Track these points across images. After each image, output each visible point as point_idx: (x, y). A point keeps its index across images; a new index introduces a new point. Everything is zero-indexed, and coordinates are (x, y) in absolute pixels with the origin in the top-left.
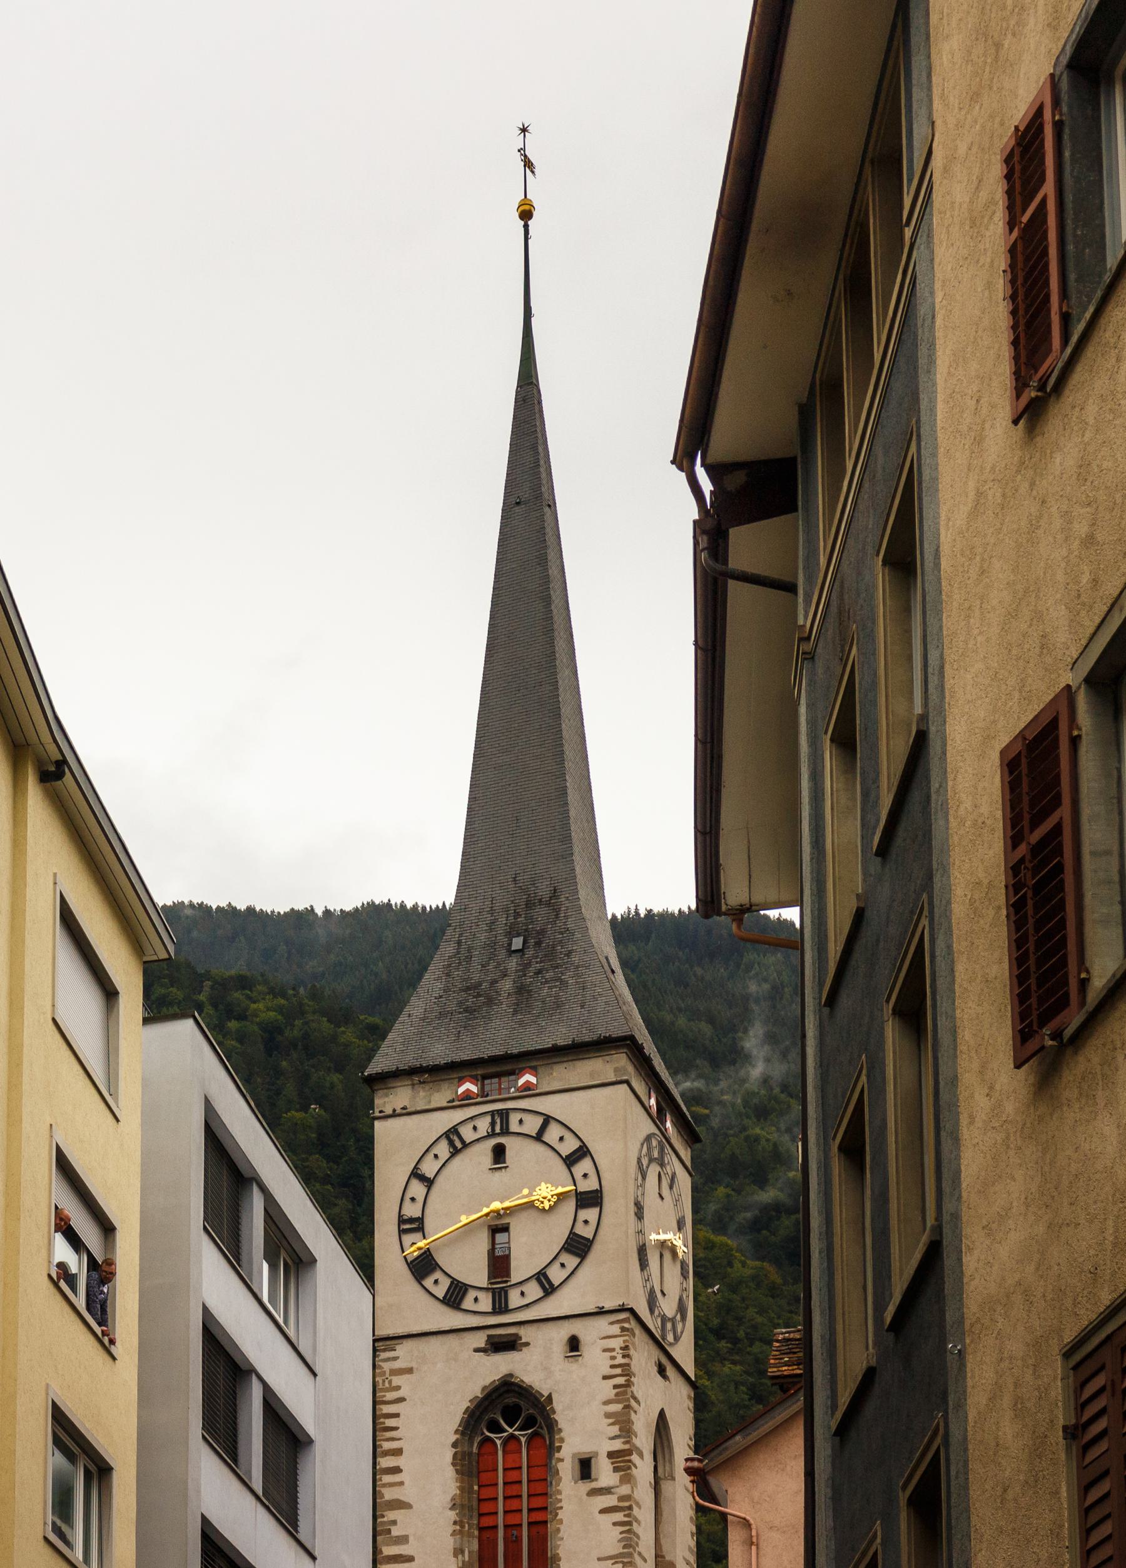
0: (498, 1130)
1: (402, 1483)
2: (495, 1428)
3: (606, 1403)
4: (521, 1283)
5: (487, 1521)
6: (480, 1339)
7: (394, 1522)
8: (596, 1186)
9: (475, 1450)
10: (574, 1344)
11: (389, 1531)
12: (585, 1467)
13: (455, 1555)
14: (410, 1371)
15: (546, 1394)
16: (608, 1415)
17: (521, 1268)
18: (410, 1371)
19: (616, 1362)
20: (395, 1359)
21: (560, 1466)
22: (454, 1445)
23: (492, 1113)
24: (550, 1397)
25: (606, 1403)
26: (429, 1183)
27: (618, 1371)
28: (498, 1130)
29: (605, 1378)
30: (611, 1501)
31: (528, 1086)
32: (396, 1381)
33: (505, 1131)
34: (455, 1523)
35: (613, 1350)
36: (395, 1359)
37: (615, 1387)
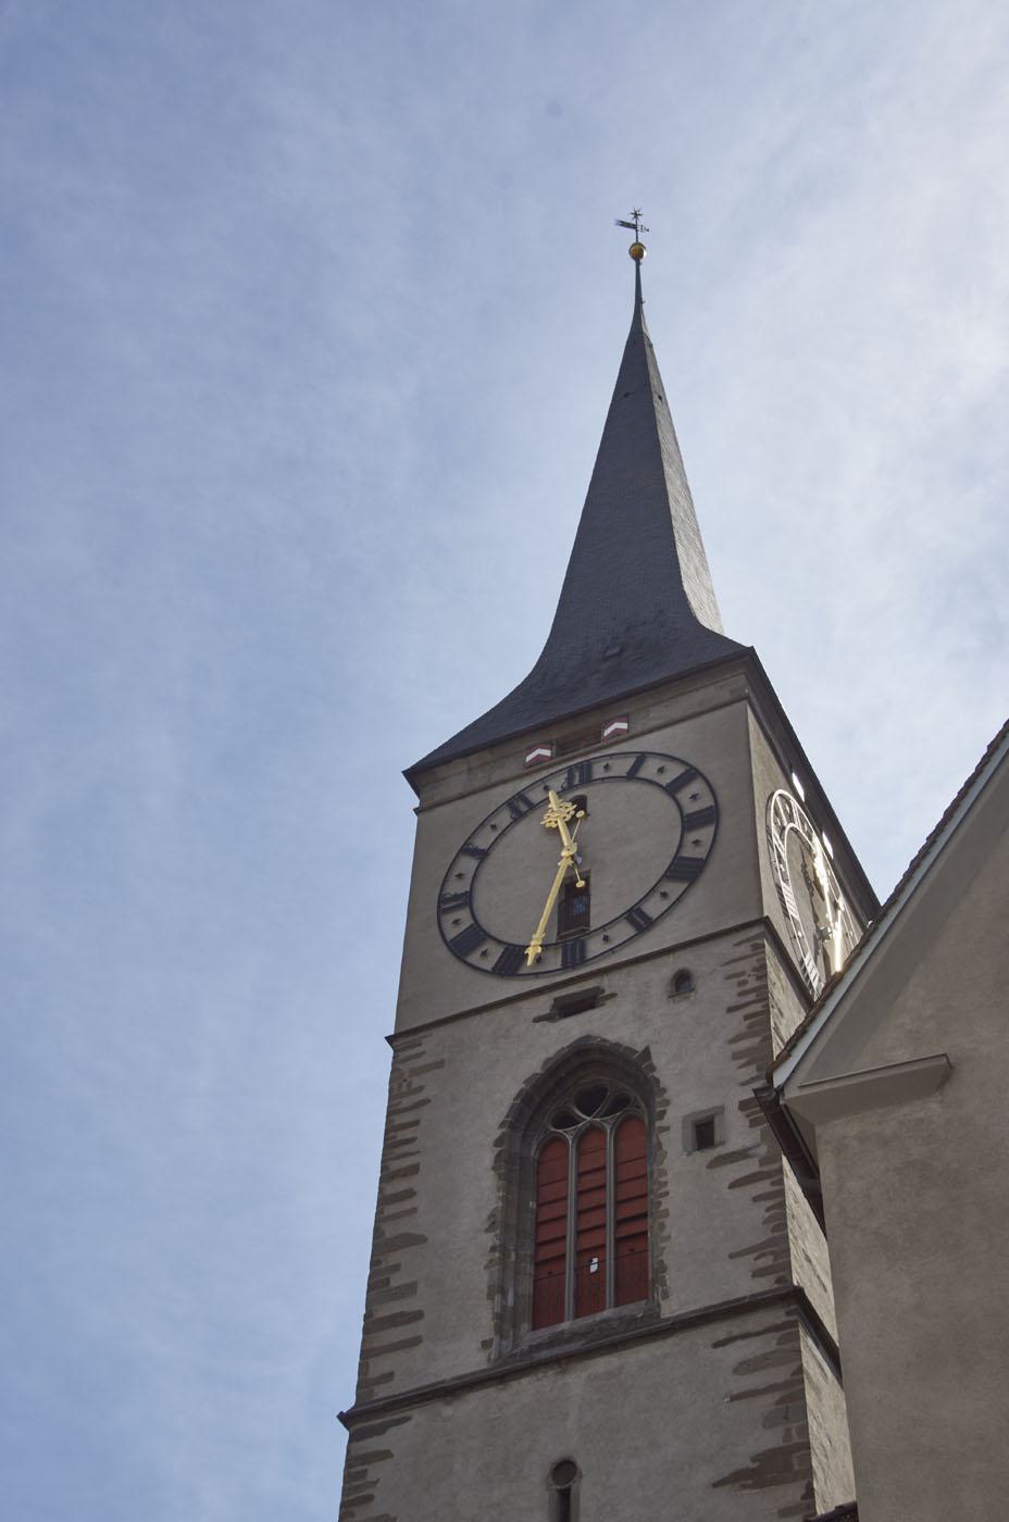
0: (576, 782)
1: (414, 1210)
2: (566, 1120)
3: (732, 1041)
4: (603, 927)
5: (547, 1252)
6: (544, 1004)
7: (396, 1268)
8: (710, 803)
9: (533, 1153)
10: (682, 983)
11: (387, 1281)
12: (704, 1133)
13: (490, 1296)
14: (440, 1064)
15: (640, 1048)
16: (736, 1056)
17: (604, 906)
18: (440, 1064)
19: (748, 987)
20: (419, 1055)
21: (663, 1137)
22: (498, 1143)
23: (570, 770)
24: (647, 1053)
25: (732, 1041)
26: (482, 855)
27: (752, 997)
28: (576, 782)
29: (730, 1010)
30: (750, 1167)
31: (617, 732)
32: (416, 1082)
33: (587, 779)
34: (493, 1249)
35: (743, 973)
36: (419, 1055)
37: (746, 1017)
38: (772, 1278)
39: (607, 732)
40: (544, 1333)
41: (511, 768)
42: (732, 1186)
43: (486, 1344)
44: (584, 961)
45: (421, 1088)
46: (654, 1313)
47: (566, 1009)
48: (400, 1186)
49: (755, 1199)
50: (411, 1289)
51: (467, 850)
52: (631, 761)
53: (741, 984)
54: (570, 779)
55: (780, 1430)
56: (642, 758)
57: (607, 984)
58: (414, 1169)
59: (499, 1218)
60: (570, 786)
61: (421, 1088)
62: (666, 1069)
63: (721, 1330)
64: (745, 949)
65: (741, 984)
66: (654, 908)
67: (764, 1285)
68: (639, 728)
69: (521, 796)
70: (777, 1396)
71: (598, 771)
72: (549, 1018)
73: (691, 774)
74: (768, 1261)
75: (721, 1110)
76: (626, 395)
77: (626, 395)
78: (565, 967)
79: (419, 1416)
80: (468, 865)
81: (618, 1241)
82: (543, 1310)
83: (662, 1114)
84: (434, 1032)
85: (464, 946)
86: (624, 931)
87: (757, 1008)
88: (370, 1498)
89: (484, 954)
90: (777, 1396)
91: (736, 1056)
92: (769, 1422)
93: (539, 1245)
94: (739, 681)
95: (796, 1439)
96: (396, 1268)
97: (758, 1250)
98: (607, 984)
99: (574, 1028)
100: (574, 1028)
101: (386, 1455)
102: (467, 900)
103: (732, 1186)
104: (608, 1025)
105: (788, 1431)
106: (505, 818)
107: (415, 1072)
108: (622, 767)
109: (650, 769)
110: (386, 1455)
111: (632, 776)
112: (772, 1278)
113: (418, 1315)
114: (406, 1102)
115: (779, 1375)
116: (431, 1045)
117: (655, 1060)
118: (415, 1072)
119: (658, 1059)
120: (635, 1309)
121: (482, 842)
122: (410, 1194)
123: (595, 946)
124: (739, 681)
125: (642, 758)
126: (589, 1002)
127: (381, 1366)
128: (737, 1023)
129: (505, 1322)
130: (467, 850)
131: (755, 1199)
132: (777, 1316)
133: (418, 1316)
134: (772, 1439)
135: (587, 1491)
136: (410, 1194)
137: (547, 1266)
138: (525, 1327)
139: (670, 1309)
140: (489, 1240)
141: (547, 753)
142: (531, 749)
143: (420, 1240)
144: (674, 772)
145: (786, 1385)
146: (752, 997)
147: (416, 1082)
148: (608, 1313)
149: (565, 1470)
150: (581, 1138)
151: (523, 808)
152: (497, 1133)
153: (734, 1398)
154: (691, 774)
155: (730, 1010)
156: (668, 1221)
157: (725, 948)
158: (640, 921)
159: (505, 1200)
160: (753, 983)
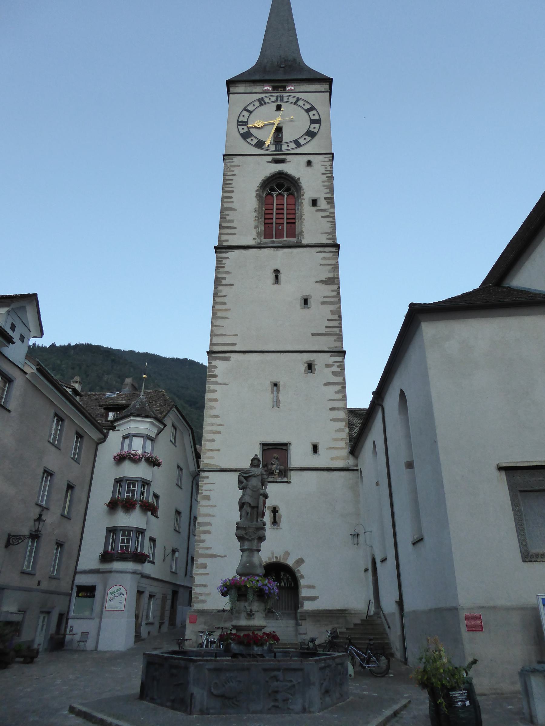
3: (323, 182)
6: (270, 158)
7: (228, 215)
10: (309, 163)
11: (226, 218)
12: (314, 203)
14: (239, 166)
17: (288, 136)
18: (239, 166)
20: (232, 162)
21: (303, 201)
22: (257, 191)
24: (299, 179)
25: (323, 182)
26: (250, 112)
27: (329, 172)
29: (322, 174)
30: (327, 214)
31: (291, 89)
32: (232, 169)
33: (282, 100)
34: (256, 217)
36: (232, 162)
39: (288, 88)
41: (258, 89)
44: (281, 150)
45: (233, 171)
47: (276, 161)
49: (328, 222)
50: (232, 221)
51: (245, 109)
52: (296, 99)
54: (277, 98)
56: (298, 99)
58: (232, 192)
59: (257, 210)
60: (276, 101)
61: (233, 171)
62: (304, 183)
63: (319, 249)
66: (302, 141)
67: (330, 242)
68: (297, 90)
70: (332, 266)
71: (285, 99)
72: (271, 162)
73: (312, 108)
74: (331, 236)
75: (320, 198)
79: (237, 251)
80: (246, 114)
83: (303, 195)
85: (246, 136)
86: (293, 145)
87: (330, 175)
88: (224, 267)
89: (252, 140)
90: (332, 266)
91: (324, 186)
92: (329, 272)
93: (265, 219)
94: (326, 86)
95: (336, 276)
96: (228, 215)
97: (329, 233)
98: (288, 158)
99: (278, 167)
100: (278, 167)
101: (228, 258)
102: (245, 123)
104: (289, 168)
105: (334, 275)
106: (257, 104)
109: (301, 103)
110: (228, 258)
111: (295, 103)
113: (235, 228)
114: (229, 173)
115: (334, 262)
116: (236, 160)
119: (302, 180)
120: (294, 240)
121: (251, 108)
123: (284, 147)
125: (298, 99)
126: (282, 161)
127: (224, 238)
128: (324, 178)
129: (259, 234)
130: (245, 109)
131: (328, 222)
132: (333, 249)
133: (235, 228)
134: (331, 275)
135: (282, 277)
141: (270, 89)
142: (264, 87)
144: (307, 106)
145: (334, 265)
147: (232, 169)
148: (285, 239)
149: (277, 271)
150: (277, 196)
151: (263, 103)
152: (257, 188)
153: (321, 265)
154: (312, 108)
155: (322, 174)
156: (304, 221)
157: (321, 157)
158: (299, 145)
160: (329, 169)
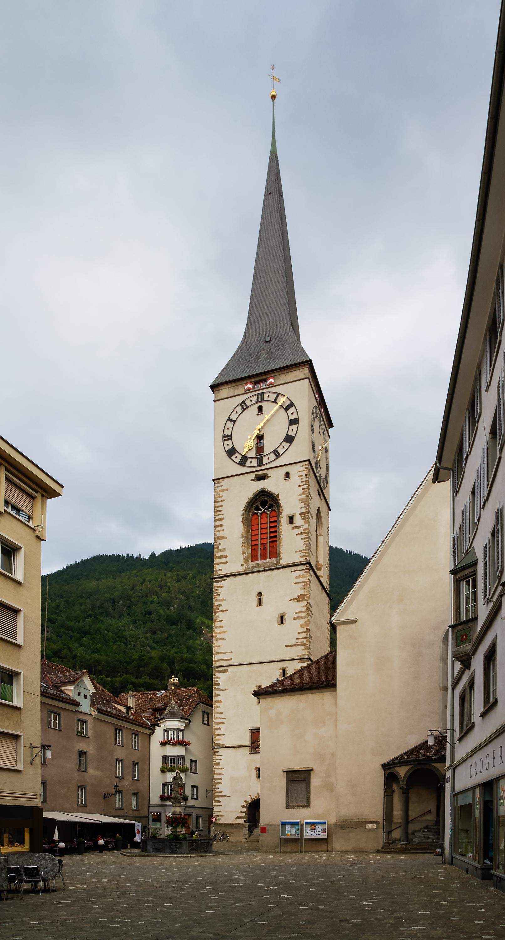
0: (260, 400)
1: (223, 530)
2: (258, 509)
3: (299, 495)
4: (267, 455)
5: (254, 543)
6: (252, 476)
7: (220, 544)
8: (296, 417)
9: (250, 517)
10: (287, 475)
11: (218, 547)
12: (291, 519)
13: (243, 554)
14: (226, 490)
15: (277, 494)
16: (300, 500)
17: (268, 447)
18: (226, 490)
19: (303, 480)
20: (221, 486)
21: (282, 520)
22: (243, 515)
23: (258, 394)
24: (278, 495)
25: (299, 495)
27: (304, 483)
28: (260, 400)
29: (299, 486)
30: (301, 530)
31: (271, 383)
32: (221, 494)
33: (262, 401)
34: (243, 543)
35: (302, 476)
36: (221, 486)
37: (303, 489)
38: (304, 558)
40: (255, 563)
41: (240, 390)
42: (297, 535)
43: (242, 565)
44: (262, 465)
45: (222, 496)
46: (278, 563)
48: (218, 523)
53: (302, 479)
55: (303, 591)
57: (269, 472)
58: (222, 519)
61: (222, 496)
64: (303, 468)
65: (302, 479)
66: (281, 451)
67: (302, 559)
69: (243, 402)
70: (303, 584)
76: (270, 194)
77: (270, 194)
78: (258, 466)
79: (228, 579)
81: (270, 542)
82: (254, 557)
84: (225, 479)
90: (303, 584)
91: (300, 500)
92: (301, 589)
93: (252, 541)
94: (306, 371)
98: (269, 472)
103: (297, 535)
107: (221, 491)
108: (273, 397)
110: (222, 587)
112: (304, 558)
113: (226, 557)
117: (280, 498)
118: (221, 491)
119: (280, 498)
120: (274, 560)
122: (221, 525)
123: (265, 460)
124: (306, 371)
129: (246, 560)
132: (304, 567)
135: (264, 598)
136: (221, 525)
137: (254, 547)
138: (250, 561)
139: (283, 562)
140: (242, 540)
143: (225, 538)
146: (304, 483)
150: (261, 514)
159: (245, 531)
